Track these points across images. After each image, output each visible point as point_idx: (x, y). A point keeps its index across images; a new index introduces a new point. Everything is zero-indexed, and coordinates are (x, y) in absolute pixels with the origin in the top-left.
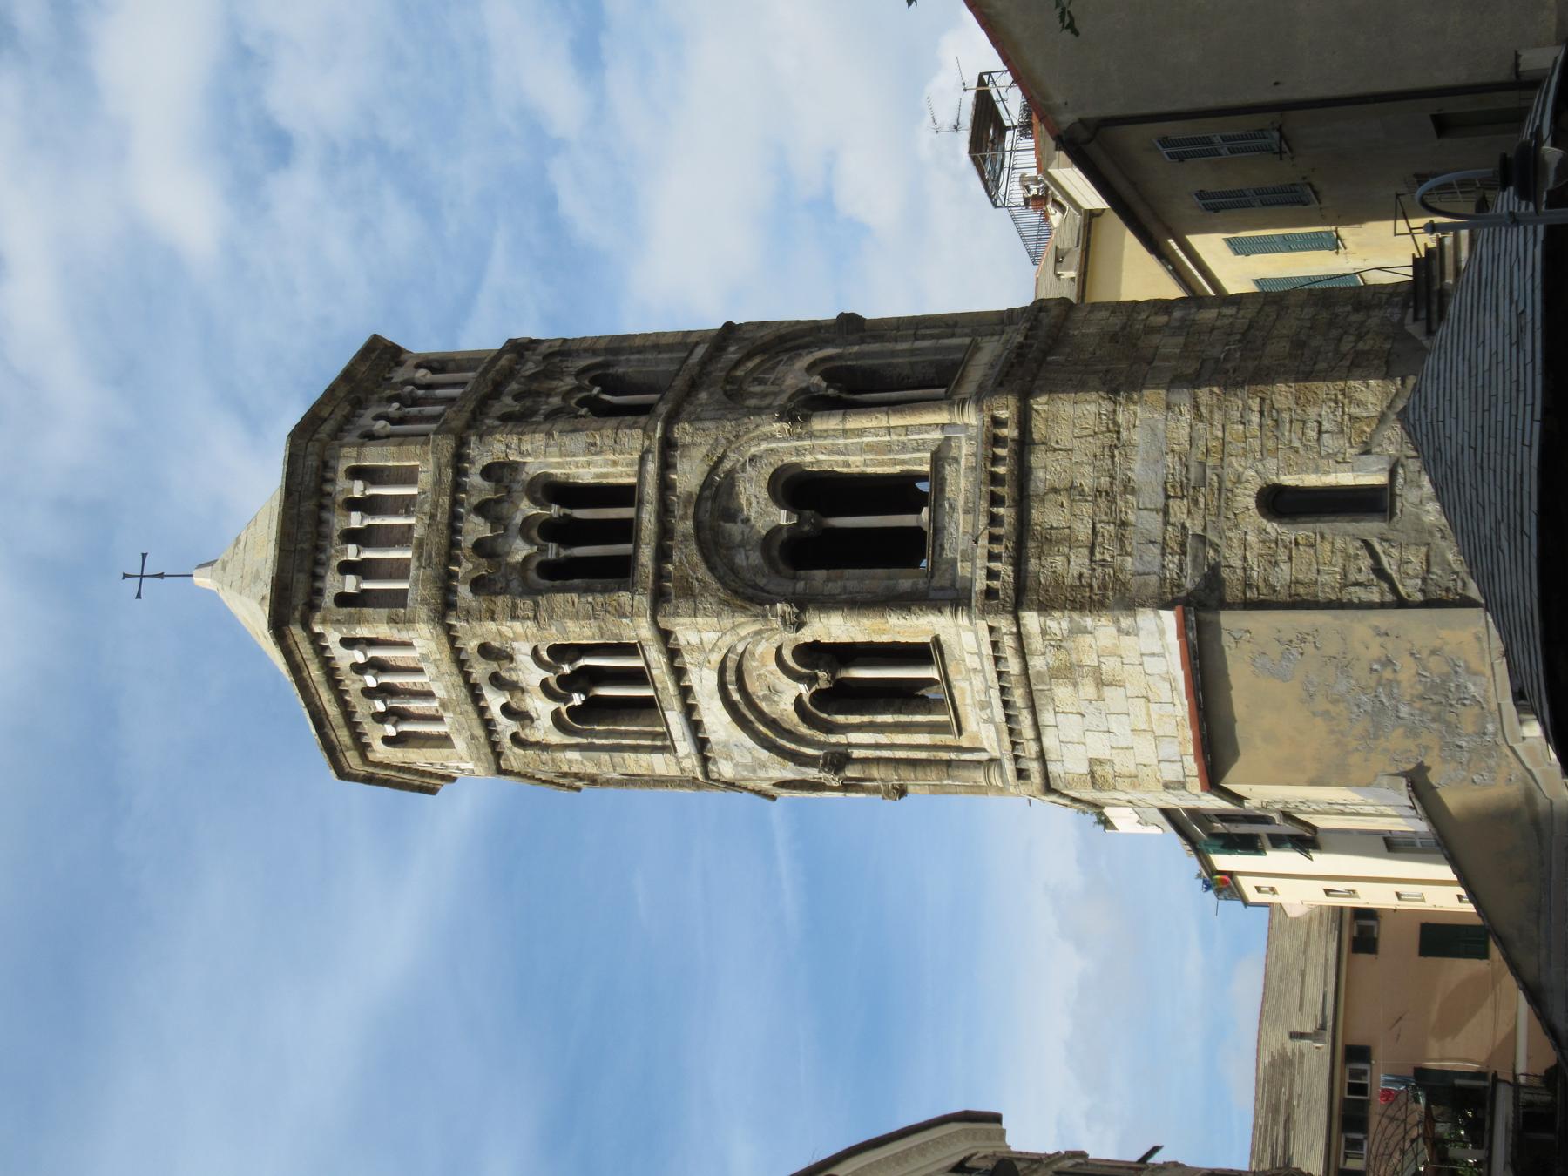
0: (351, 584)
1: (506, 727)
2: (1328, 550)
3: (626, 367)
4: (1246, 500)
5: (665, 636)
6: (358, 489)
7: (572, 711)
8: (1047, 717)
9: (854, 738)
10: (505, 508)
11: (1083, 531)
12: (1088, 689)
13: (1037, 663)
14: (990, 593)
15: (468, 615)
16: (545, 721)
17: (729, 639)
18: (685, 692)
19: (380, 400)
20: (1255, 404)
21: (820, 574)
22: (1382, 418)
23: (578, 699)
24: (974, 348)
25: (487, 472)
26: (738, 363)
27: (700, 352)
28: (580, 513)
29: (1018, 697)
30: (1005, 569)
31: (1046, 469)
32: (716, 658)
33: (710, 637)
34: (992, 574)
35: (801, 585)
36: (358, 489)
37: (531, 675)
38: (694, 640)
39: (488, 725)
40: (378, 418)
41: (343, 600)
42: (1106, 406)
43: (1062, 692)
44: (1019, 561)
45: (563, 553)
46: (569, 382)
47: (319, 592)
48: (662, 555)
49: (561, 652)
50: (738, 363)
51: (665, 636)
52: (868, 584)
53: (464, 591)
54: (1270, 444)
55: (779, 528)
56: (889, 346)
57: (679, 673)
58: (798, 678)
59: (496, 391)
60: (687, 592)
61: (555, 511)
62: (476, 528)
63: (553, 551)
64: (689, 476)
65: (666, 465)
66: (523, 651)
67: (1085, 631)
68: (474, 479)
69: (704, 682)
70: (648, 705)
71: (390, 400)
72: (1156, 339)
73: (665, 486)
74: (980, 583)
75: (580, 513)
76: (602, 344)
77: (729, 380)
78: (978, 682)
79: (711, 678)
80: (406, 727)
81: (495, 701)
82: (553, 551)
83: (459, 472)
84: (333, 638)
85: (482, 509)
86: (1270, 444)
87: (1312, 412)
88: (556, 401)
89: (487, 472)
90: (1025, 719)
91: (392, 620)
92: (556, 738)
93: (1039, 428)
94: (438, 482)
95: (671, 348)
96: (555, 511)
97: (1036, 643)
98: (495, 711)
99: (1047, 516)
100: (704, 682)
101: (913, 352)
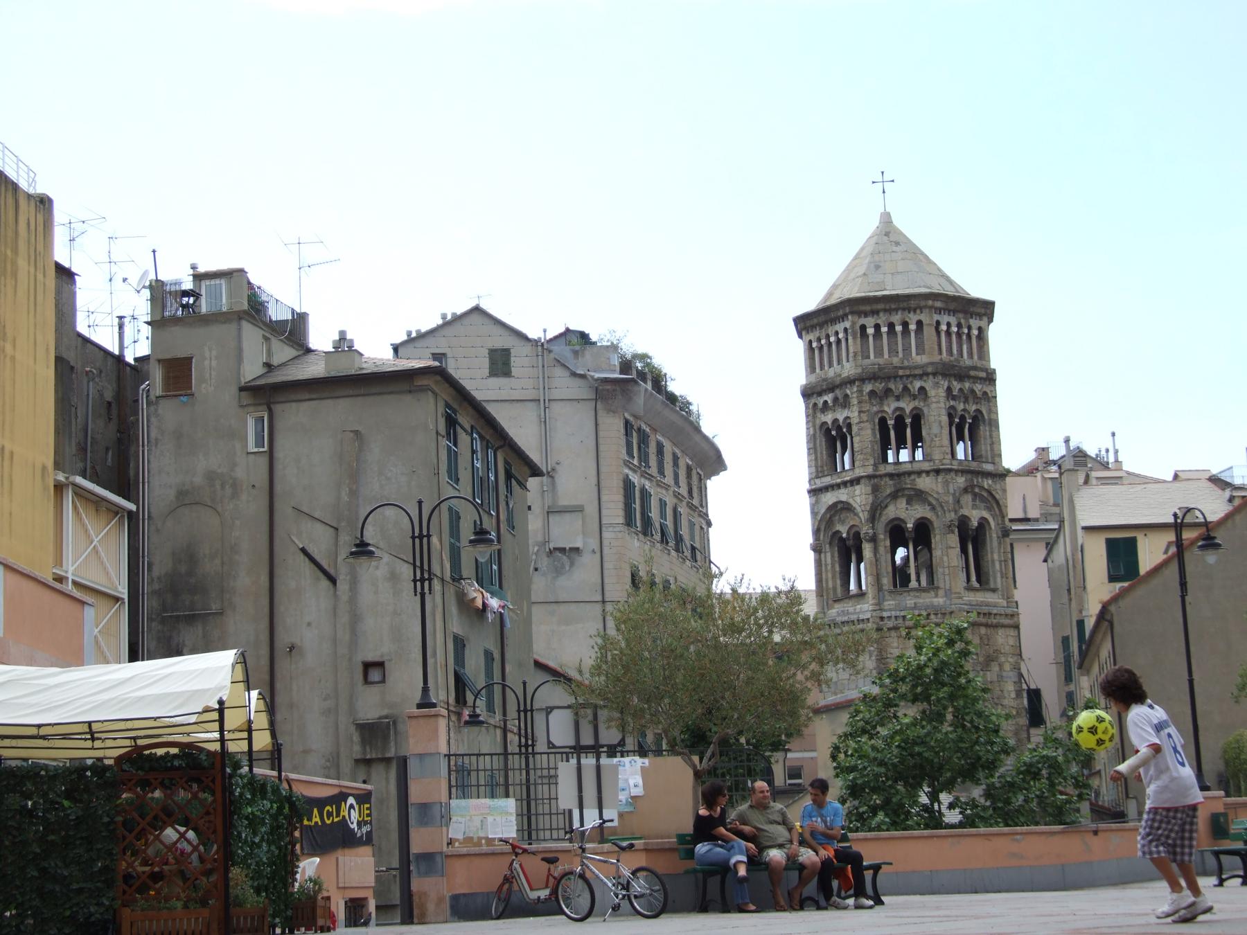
0: (870, 331)
1: (820, 401)
3: (983, 430)
5: (856, 481)
6: (913, 327)
9: (829, 555)
14: (882, 618)
15: (860, 391)
17: (859, 509)
18: (838, 486)
19: (958, 319)
23: (834, 433)
24: (994, 590)
25: (922, 389)
26: (982, 488)
27: (988, 467)
28: (909, 431)
30: (890, 624)
32: (851, 501)
33: (858, 500)
34: (889, 617)
35: (882, 537)
36: (913, 327)
37: (841, 415)
38: (857, 492)
39: (820, 394)
41: (863, 328)
47: (866, 316)
49: (849, 426)
51: (856, 481)
52: (883, 564)
53: (868, 388)
56: (996, 550)
57: (845, 484)
58: (848, 533)
59: (961, 377)
60: (875, 490)
61: (908, 421)
62: (896, 387)
63: (891, 422)
65: (928, 473)
66: (845, 413)
68: (918, 384)
69: (842, 495)
72: (996, 669)
74: (885, 614)
75: (909, 431)
76: (993, 416)
77: (973, 486)
79: (844, 498)
80: (817, 352)
81: (829, 398)
82: (891, 422)
83: (921, 377)
84: (847, 324)
85: (906, 389)
89: (922, 389)
91: (855, 354)
92: (818, 422)
94: (916, 367)
95: (992, 450)
96: (908, 421)
98: (826, 398)
100: (842, 495)
101: (993, 561)
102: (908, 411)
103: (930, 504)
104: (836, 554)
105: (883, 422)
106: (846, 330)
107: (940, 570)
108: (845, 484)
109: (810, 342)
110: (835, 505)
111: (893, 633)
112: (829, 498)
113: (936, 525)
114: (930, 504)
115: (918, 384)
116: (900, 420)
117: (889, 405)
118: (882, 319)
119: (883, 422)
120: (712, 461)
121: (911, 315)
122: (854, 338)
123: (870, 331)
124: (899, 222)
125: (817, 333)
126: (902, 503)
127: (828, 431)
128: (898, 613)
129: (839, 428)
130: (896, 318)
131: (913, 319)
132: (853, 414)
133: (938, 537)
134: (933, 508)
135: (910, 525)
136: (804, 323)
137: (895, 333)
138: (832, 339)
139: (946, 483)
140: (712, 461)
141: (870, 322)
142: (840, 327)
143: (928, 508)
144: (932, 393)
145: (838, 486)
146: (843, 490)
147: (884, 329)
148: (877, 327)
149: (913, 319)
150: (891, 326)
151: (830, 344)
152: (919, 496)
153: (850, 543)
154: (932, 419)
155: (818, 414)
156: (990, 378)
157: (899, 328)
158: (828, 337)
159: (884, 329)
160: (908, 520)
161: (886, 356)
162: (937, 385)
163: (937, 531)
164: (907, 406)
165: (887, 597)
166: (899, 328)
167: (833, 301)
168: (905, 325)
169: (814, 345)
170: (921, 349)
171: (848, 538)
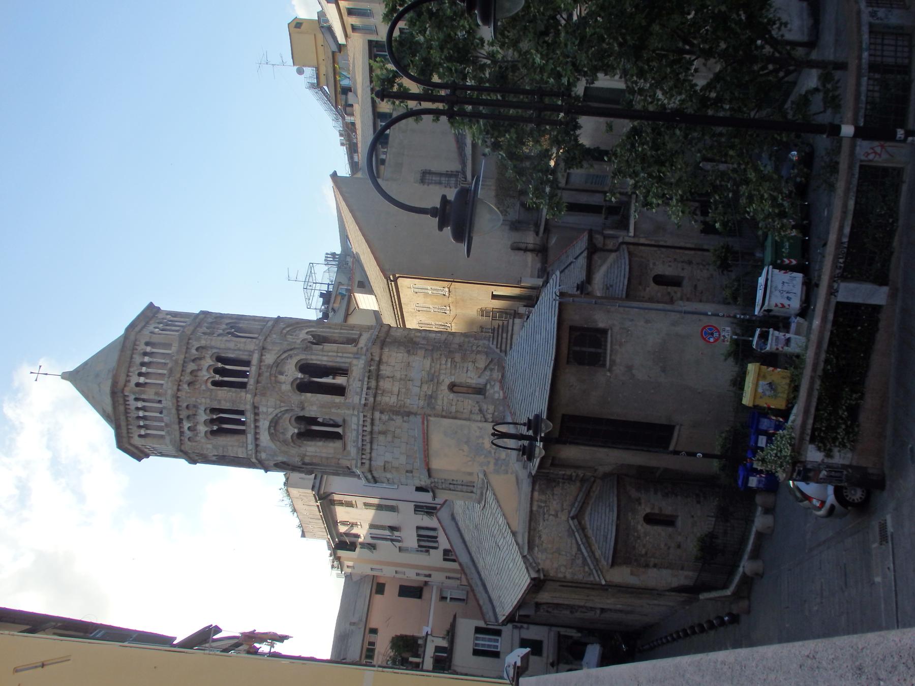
0: (142, 380)
1: (188, 434)
2: (468, 403)
4: (444, 387)
6: (148, 349)
7: (213, 433)
8: (375, 447)
10: (202, 362)
11: (396, 390)
12: (389, 438)
13: (376, 429)
14: (365, 405)
16: (203, 434)
18: (256, 427)
20: (449, 360)
21: (309, 395)
22: (485, 368)
23: (215, 428)
24: (361, 335)
25: (197, 349)
26: (284, 329)
27: (270, 324)
29: (368, 438)
30: (371, 399)
31: (385, 370)
32: (270, 417)
36: (148, 349)
37: (203, 417)
38: (265, 410)
39: (182, 433)
40: (155, 328)
42: (406, 355)
43: (381, 438)
44: (375, 397)
45: (221, 379)
46: (224, 326)
47: (129, 381)
48: (258, 382)
49: (213, 410)
50: (284, 329)
54: (453, 372)
55: (297, 378)
57: (256, 421)
59: (199, 325)
61: (220, 365)
62: (191, 366)
63: (218, 377)
64: (269, 358)
65: (262, 355)
67: (393, 420)
69: (264, 424)
70: (243, 432)
71: (159, 323)
73: (261, 360)
78: (354, 433)
79: (267, 424)
81: (186, 425)
82: (218, 377)
86: (453, 372)
87: (466, 365)
88: (221, 331)
90: (368, 447)
93: (385, 359)
96: (220, 365)
97: (377, 422)
98: (186, 428)
99: (385, 384)
100: (264, 424)
102: (212, 363)
103: (287, 358)
104: (309, 443)
105: (215, 384)
106: (137, 399)
107: (338, 359)
108: (256, 421)
109: (140, 436)
110: (270, 434)
111: (379, 398)
112: (265, 438)
113: (303, 357)
114: (287, 358)
115: (194, 351)
116: (217, 371)
117: (204, 376)
118: (135, 370)
119: (215, 384)
120: (151, 312)
121: (139, 348)
122: (143, 392)
123: (142, 380)
124: (71, 368)
125: (134, 429)
126: (282, 378)
127: (213, 433)
128: (364, 393)
129: (212, 421)
130: (138, 359)
131: (142, 347)
132: (204, 402)
133: (313, 357)
134: (291, 357)
135: (300, 375)
136: (125, 443)
137: (150, 363)
138: (141, 414)
139: (274, 343)
140: (151, 312)
141: (135, 379)
142: (133, 404)
143: (289, 360)
144: (203, 343)
145: (256, 427)
146: (260, 424)
147: (144, 369)
148: (140, 374)
149: (142, 347)
150: (143, 364)
151: (144, 418)
152: (278, 365)
153: (303, 428)
154: (223, 346)
155: (198, 439)
156: (205, 314)
157: (147, 359)
158: (139, 418)
159: (144, 369)
160: (295, 376)
161: (165, 372)
162: (198, 339)
163: (309, 357)
164: (208, 362)
165: (350, 401)
166: (147, 359)
167: (109, 409)
168: (145, 354)
169: (143, 432)
170: (167, 346)
171: (299, 429)
